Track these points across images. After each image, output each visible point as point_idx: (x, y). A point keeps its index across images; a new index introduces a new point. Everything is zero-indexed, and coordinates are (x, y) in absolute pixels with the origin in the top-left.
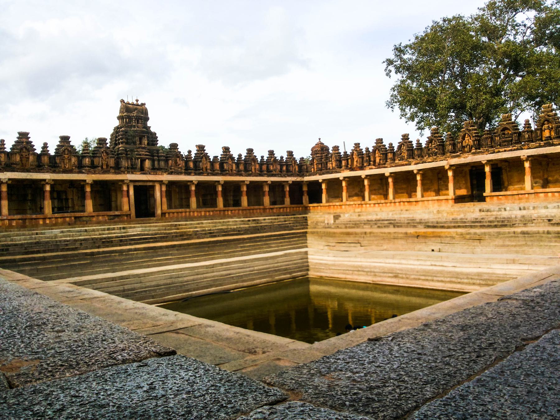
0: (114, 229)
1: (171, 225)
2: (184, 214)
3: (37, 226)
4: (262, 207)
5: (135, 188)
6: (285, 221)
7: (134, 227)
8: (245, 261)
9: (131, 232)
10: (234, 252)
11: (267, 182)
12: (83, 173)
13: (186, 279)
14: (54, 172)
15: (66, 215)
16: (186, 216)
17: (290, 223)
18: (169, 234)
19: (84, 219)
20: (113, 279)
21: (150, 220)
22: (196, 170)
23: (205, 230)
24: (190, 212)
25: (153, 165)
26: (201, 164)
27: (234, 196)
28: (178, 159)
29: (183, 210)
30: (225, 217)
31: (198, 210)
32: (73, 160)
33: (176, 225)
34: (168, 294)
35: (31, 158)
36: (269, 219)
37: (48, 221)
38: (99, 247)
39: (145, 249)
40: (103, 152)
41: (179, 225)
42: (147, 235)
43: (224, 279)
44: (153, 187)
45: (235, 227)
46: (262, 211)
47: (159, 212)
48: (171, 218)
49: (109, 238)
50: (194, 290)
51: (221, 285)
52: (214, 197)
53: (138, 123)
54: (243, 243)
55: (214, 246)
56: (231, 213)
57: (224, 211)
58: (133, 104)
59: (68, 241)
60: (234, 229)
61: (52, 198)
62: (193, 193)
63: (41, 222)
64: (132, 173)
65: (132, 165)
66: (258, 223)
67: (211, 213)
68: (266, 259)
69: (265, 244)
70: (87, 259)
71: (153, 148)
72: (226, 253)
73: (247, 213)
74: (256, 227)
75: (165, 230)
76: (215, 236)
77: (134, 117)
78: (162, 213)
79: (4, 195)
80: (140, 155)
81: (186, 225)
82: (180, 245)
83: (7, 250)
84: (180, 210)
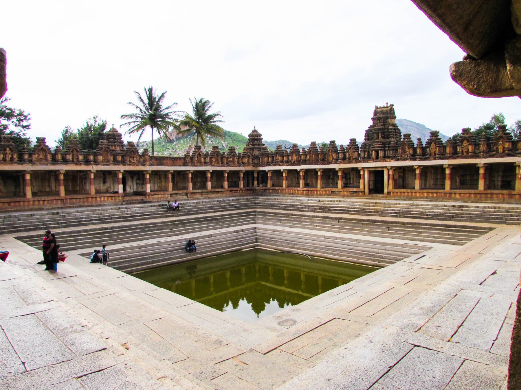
0: (334, 201)
1: (372, 203)
2: (406, 194)
3: (312, 195)
4: (505, 192)
5: (370, 173)
6: (508, 212)
7: (346, 202)
8: (357, 241)
9: (341, 204)
10: (376, 232)
11: (515, 163)
12: (337, 163)
14: (323, 164)
15: (326, 189)
17: (511, 216)
18: (364, 209)
19: (336, 192)
20: (273, 231)
21: (377, 196)
22: (423, 156)
23: (395, 210)
24: (412, 193)
25: (385, 154)
26: (428, 149)
27: (503, 177)
28: (406, 147)
29: (405, 190)
30: (450, 199)
31: (420, 191)
32: (334, 155)
33: (376, 203)
34: (283, 246)
36: (485, 207)
37: (318, 193)
38: (314, 212)
39: (322, 217)
40: (350, 149)
41: (379, 203)
42: (348, 208)
43: (323, 249)
44: (383, 171)
45: (427, 211)
46: (506, 196)
47: (386, 191)
48: (394, 196)
49: (326, 207)
50: (297, 249)
51: (315, 251)
52: (475, 177)
53: (380, 122)
54: (397, 226)
55: (367, 224)
56: (460, 196)
57: (451, 193)
58: (384, 108)
59: (305, 206)
60: (425, 212)
61: (342, 178)
62: (417, 176)
63: (316, 193)
64: (368, 162)
65: (368, 155)
66: (462, 210)
67: (435, 195)
68: (379, 243)
69: (417, 232)
70: (289, 217)
71: (388, 140)
72: (368, 231)
73: (480, 198)
74: (454, 213)
75: (364, 206)
76: (396, 216)
77: (384, 118)
78: (388, 192)
79: (301, 177)
80: (374, 148)
81: (384, 204)
82: (345, 219)
84: (402, 190)
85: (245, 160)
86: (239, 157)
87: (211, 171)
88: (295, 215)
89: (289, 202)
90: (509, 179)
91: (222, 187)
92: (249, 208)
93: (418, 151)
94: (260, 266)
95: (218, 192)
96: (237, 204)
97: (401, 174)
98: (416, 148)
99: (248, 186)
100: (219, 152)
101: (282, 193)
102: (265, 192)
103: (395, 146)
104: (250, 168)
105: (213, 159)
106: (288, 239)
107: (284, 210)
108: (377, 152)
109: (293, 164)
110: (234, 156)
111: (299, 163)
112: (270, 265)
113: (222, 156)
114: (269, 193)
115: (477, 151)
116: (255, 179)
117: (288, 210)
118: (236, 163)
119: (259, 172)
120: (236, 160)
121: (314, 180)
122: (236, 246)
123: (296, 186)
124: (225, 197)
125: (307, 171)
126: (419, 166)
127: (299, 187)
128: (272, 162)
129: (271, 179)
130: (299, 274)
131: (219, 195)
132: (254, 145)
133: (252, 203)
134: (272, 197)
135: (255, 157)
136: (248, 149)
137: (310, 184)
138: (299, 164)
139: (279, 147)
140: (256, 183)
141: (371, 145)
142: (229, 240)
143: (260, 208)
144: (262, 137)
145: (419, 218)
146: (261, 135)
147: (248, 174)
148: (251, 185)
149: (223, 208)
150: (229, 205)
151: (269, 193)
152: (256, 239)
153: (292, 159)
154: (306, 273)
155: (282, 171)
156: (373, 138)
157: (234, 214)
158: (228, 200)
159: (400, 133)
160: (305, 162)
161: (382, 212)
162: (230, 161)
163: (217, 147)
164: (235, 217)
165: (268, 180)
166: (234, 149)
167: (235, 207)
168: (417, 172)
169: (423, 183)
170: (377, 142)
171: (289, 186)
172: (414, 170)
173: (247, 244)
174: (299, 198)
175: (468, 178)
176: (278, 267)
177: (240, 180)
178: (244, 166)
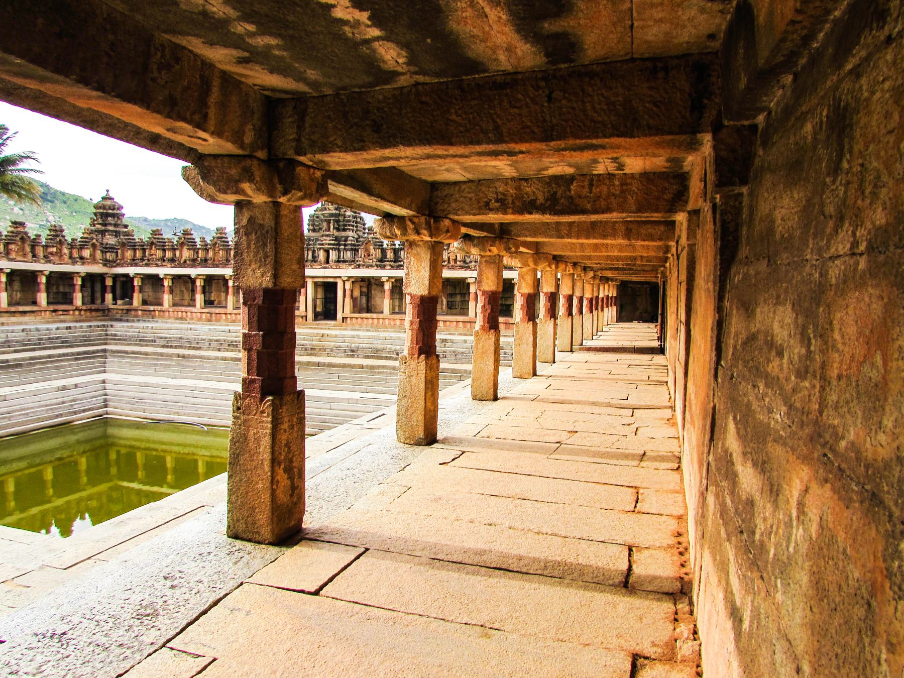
3: (218, 321)
5: (316, 285)
13: (193, 400)
16: (373, 323)
25: (339, 257)
26: (402, 252)
29: (368, 315)
34: (157, 412)
35: (221, 252)
37: (229, 317)
47: (340, 315)
50: (184, 415)
63: (224, 316)
65: (313, 257)
71: (344, 234)
76: (353, 356)
79: (199, 289)
83: (155, 341)
84: (364, 315)
85: (86, 253)
86: (72, 246)
87: (8, 271)
88: (184, 357)
89: (174, 334)
90: (508, 303)
91: (34, 303)
92: (93, 345)
93: (390, 255)
94: (118, 452)
95: (24, 313)
96: (66, 337)
97: (365, 290)
98: (386, 249)
99: (93, 302)
100: (26, 233)
101: (163, 317)
102: (128, 314)
103: (354, 245)
104: (97, 269)
105: (12, 247)
106: (168, 398)
107: (163, 346)
108: (327, 252)
109: (184, 265)
110: (61, 243)
111: (194, 263)
112: (139, 448)
113: (35, 243)
114: (137, 316)
115: (468, 260)
116: (109, 289)
117: (171, 347)
118: (66, 258)
119: (115, 277)
120: (66, 251)
121: (223, 295)
122: (61, 415)
123: (189, 305)
124: (42, 323)
125: (209, 279)
126: (390, 278)
127: (195, 306)
128: (142, 260)
129: (140, 292)
130: (196, 461)
131: (26, 319)
132: (105, 225)
133: (100, 335)
134: (141, 324)
135: (106, 249)
136: (92, 232)
137: (216, 302)
138: (193, 266)
139: (155, 233)
140: (109, 297)
141: (317, 240)
142: (47, 406)
143: (116, 344)
144: (123, 211)
145: (387, 358)
146: (121, 208)
147: (91, 280)
148: (99, 301)
149: (35, 344)
150: (49, 339)
151: (137, 316)
152: (106, 400)
153: (181, 256)
154: (206, 458)
155: (161, 276)
156: (320, 229)
157: (60, 355)
158: (48, 329)
159: (364, 225)
160: (205, 262)
161: (332, 350)
162: (52, 253)
163: (22, 224)
164: (62, 360)
165: (133, 291)
166: (62, 231)
167: (63, 342)
168: (387, 286)
169: (397, 304)
170: (327, 236)
171: (175, 305)
172: (382, 284)
173: (84, 411)
174: (190, 326)
175: (458, 298)
176: (154, 453)
177: (74, 291)
178: (83, 263)
